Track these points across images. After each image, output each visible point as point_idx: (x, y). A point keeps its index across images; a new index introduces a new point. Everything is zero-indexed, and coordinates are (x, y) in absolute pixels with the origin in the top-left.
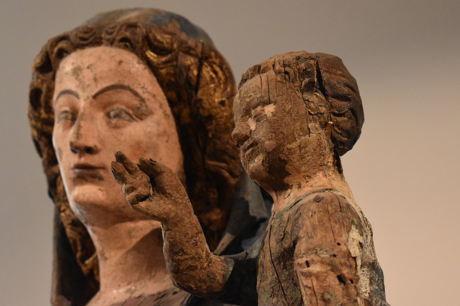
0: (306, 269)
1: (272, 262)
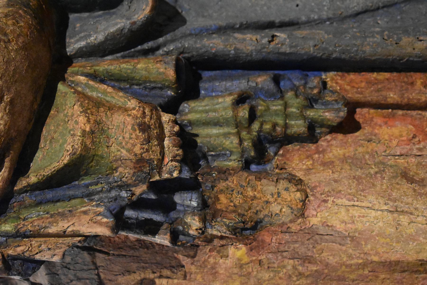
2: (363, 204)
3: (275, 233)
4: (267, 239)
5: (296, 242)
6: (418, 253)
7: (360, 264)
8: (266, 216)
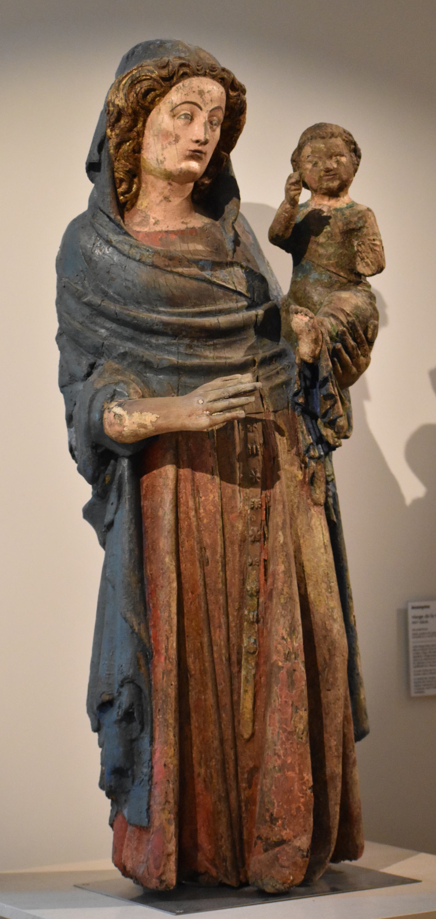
0: (374, 242)
1: (341, 233)
3: (306, 492)
4: (305, 489)
6: (308, 560)
8: (315, 487)
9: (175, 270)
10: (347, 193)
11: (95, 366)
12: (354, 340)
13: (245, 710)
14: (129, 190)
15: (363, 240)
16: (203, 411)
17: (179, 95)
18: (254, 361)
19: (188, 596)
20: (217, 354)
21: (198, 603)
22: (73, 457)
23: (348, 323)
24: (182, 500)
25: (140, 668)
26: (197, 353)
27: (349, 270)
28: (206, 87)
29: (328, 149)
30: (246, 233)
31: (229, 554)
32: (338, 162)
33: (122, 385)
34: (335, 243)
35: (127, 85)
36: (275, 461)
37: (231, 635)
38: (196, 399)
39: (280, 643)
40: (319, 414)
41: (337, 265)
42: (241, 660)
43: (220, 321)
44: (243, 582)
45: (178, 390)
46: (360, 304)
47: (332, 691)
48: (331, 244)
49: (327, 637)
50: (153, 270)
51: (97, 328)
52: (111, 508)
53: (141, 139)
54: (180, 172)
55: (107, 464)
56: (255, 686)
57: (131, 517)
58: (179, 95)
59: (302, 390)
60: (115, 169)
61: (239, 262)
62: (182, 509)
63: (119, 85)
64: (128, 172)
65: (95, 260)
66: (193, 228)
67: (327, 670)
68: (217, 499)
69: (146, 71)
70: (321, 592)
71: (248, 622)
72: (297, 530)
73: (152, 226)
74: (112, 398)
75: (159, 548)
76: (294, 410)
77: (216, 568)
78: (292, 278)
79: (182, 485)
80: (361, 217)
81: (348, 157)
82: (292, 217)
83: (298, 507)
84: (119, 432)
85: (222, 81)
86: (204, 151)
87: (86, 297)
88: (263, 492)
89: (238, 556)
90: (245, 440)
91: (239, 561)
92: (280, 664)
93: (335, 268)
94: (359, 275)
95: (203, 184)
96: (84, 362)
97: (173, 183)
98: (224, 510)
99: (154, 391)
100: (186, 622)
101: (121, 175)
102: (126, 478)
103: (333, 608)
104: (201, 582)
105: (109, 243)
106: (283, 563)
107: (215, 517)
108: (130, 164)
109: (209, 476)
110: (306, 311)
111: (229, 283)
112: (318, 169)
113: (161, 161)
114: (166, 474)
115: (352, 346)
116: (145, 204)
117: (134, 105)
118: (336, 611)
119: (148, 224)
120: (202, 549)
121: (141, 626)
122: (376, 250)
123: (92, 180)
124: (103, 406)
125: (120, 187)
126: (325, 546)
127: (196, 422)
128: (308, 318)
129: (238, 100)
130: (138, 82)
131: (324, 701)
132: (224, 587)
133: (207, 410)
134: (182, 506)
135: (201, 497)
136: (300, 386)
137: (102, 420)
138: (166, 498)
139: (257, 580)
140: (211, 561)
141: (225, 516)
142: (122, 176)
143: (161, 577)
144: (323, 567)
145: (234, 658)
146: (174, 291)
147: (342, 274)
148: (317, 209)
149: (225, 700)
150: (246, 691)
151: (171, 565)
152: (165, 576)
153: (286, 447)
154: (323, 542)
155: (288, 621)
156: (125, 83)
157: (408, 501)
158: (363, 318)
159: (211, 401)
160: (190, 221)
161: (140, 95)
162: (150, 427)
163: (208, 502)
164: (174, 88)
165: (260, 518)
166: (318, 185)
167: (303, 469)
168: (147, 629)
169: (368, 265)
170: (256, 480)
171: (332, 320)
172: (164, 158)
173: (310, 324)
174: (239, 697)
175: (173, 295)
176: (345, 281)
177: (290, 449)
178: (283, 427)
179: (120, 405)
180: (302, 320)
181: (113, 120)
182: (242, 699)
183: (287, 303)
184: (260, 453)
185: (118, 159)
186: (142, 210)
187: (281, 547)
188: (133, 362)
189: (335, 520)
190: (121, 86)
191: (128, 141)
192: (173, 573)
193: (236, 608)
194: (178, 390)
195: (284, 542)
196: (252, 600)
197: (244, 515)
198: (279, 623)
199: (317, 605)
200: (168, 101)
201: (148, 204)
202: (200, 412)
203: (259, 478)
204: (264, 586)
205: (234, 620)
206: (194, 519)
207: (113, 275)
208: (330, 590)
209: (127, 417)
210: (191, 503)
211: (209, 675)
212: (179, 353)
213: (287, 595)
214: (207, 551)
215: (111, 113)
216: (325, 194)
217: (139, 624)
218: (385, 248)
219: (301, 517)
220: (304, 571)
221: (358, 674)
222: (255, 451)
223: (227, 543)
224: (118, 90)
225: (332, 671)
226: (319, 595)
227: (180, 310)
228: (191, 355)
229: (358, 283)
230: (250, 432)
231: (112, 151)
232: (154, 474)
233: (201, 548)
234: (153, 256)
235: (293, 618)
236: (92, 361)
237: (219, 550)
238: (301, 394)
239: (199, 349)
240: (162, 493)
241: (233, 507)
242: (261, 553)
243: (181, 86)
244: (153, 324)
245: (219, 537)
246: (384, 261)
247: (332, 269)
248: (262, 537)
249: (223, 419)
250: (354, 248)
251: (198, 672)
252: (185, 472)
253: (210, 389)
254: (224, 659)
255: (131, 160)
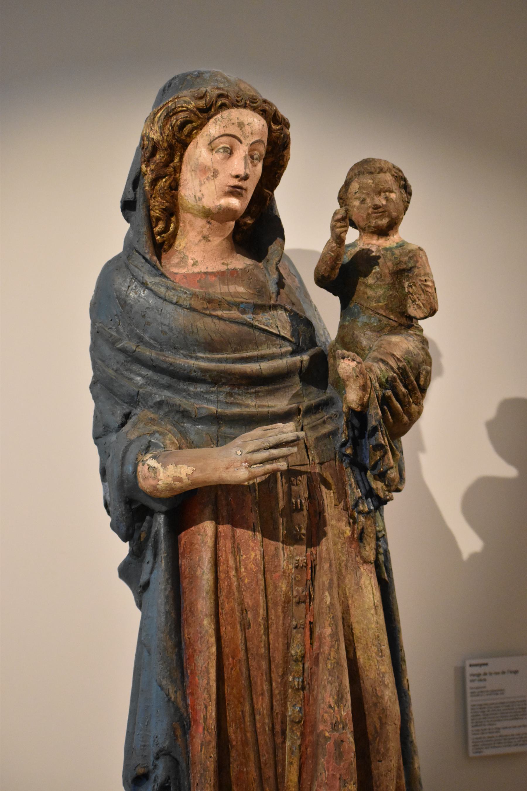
1: (390, 274)
2: (374, 591)
3: (355, 549)
4: (353, 546)
5: (352, 561)
6: (357, 622)
7: (346, 595)
8: (364, 544)
9: (214, 313)
10: (397, 232)
11: (130, 416)
12: (406, 387)
13: (290, 783)
14: (166, 229)
15: (414, 281)
16: (242, 463)
17: (218, 127)
18: (299, 410)
19: (228, 662)
20: (259, 402)
21: (240, 669)
22: (109, 512)
23: (399, 368)
24: (222, 559)
25: (176, 739)
26: (238, 401)
27: (399, 313)
28: (246, 119)
29: (377, 185)
30: (292, 275)
31: (272, 617)
32: (387, 199)
33: (157, 435)
34: (384, 284)
35: (162, 117)
36: (321, 517)
37: (275, 703)
38: (234, 450)
39: (326, 712)
40: (368, 466)
41: (387, 307)
42: (286, 730)
43: (262, 367)
44: (288, 646)
45: (218, 441)
46: (411, 348)
47: (383, 762)
48: (381, 285)
49: (378, 705)
50: (191, 313)
51: (132, 376)
52: (147, 568)
53: (178, 175)
54: (219, 209)
55: (143, 520)
56: (301, 758)
57: (167, 577)
58: (218, 127)
59: (350, 440)
60: (151, 208)
61: (283, 305)
62: (222, 568)
63: (154, 118)
64: (164, 210)
65: (130, 303)
66: (234, 270)
67: (378, 739)
68: (258, 557)
69: (182, 102)
70: (371, 656)
71: (292, 689)
72: (345, 590)
73: (190, 267)
74: (147, 450)
75: (197, 610)
76: (342, 462)
77: (259, 631)
78: (340, 322)
79: (221, 542)
80: (412, 257)
81: (398, 194)
82: (338, 257)
83: (346, 566)
84: (153, 486)
85: (264, 113)
86: (244, 187)
87: (120, 344)
88: (308, 549)
89: (281, 618)
90: (289, 494)
91: (283, 623)
92: (327, 734)
93: (385, 311)
94: (411, 318)
95: (246, 224)
96: (119, 412)
97: (212, 221)
98: (266, 570)
99: (192, 442)
100: (227, 689)
101: (157, 213)
102: (162, 535)
103: (384, 673)
104: (242, 647)
105: (144, 285)
106: (330, 626)
107: (257, 577)
108: (167, 202)
109: (251, 533)
110: (354, 356)
111: (272, 327)
112: (366, 205)
113: (199, 198)
114: (205, 531)
115: (403, 393)
116: (183, 244)
117: (170, 139)
118: (387, 676)
119: (186, 264)
120: (243, 611)
121: (178, 694)
122: (428, 291)
123: (128, 220)
124: (137, 458)
125: (156, 226)
126: (376, 607)
127: (234, 475)
128: (355, 363)
129: (282, 133)
130: (174, 114)
131: (375, 772)
132: (266, 652)
133: (245, 462)
134: (222, 564)
135: (242, 556)
136: (348, 436)
137: (136, 473)
138: (204, 556)
139: (302, 644)
140: (253, 624)
141: (268, 576)
142: (158, 215)
143: (199, 642)
144: (373, 629)
145: (278, 728)
146: (213, 335)
147: (392, 317)
148: (366, 249)
149: (269, 773)
150: (291, 763)
151: (210, 628)
152: (203, 640)
153: (333, 501)
154: (373, 602)
155: (336, 688)
156: (161, 116)
157: (465, 555)
158: (415, 363)
159: (250, 452)
160: (231, 262)
161: (176, 128)
162: (186, 480)
163: (249, 561)
164: (212, 120)
165: (305, 578)
166: (366, 223)
167: (352, 524)
168: (184, 697)
169: (420, 307)
170: (300, 536)
171: (381, 365)
172: (202, 195)
173: (358, 370)
174: (284, 769)
175: (212, 339)
176: (395, 324)
177: (337, 503)
178: (330, 480)
179: (154, 457)
180: (349, 365)
181: (147, 155)
182: (286, 772)
183: (335, 349)
184: (304, 507)
185: (153, 196)
186: (180, 250)
187: (328, 609)
188: (170, 412)
189: (387, 578)
190: (156, 119)
191: (164, 177)
192: (212, 637)
193: (280, 674)
194: (218, 441)
195: (330, 603)
196: (297, 665)
197: (287, 575)
198: (326, 691)
199: (367, 670)
200: (206, 133)
201: (187, 244)
202: (239, 464)
203: (304, 535)
204: (310, 650)
205: (277, 688)
206: (234, 579)
207: (149, 319)
208: (380, 654)
209: (161, 470)
210: (231, 562)
211: (251, 746)
212: (218, 401)
213: (335, 660)
214: (249, 612)
215: (145, 147)
216: (373, 233)
217: (176, 692)
218: (437, 290)
219: (349, 576)
220: (353, 634)
221: (412, 742)
222: (299, 506)
223: (270, 605)
224: (153, 122)
225: (383, 741)
226: (369, 659)
227: (220, 356)
228: (231, 403)
229: (409, 327)
230: (294, 485)
231: (147, 188)
232: (192, 530)
233: (242, 610)
234: (191, 299)
235: (341, 684)
236: (128, 410)
237: (262, 611)
238: (348, 445)
239: (240, 397)
240: (201, 551)
241: (276, 566)
242: (307, 614)
243: (220, 118)
244: (191, 371)
245: (261, 598)
246: (437, 302)
247: (382, 312)
248: (308, 597)
249: (263, 471)
250: (405, 290)
251: (239, 743)
252: (225, 529)
253: (250, 439)
254: (267, 729)
255: (168, 197)
